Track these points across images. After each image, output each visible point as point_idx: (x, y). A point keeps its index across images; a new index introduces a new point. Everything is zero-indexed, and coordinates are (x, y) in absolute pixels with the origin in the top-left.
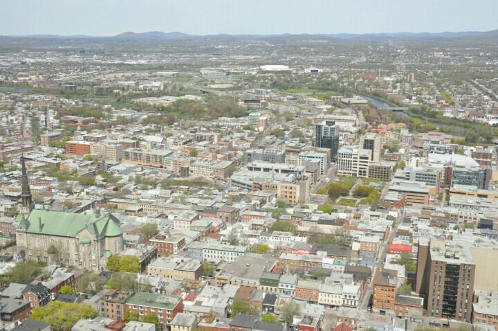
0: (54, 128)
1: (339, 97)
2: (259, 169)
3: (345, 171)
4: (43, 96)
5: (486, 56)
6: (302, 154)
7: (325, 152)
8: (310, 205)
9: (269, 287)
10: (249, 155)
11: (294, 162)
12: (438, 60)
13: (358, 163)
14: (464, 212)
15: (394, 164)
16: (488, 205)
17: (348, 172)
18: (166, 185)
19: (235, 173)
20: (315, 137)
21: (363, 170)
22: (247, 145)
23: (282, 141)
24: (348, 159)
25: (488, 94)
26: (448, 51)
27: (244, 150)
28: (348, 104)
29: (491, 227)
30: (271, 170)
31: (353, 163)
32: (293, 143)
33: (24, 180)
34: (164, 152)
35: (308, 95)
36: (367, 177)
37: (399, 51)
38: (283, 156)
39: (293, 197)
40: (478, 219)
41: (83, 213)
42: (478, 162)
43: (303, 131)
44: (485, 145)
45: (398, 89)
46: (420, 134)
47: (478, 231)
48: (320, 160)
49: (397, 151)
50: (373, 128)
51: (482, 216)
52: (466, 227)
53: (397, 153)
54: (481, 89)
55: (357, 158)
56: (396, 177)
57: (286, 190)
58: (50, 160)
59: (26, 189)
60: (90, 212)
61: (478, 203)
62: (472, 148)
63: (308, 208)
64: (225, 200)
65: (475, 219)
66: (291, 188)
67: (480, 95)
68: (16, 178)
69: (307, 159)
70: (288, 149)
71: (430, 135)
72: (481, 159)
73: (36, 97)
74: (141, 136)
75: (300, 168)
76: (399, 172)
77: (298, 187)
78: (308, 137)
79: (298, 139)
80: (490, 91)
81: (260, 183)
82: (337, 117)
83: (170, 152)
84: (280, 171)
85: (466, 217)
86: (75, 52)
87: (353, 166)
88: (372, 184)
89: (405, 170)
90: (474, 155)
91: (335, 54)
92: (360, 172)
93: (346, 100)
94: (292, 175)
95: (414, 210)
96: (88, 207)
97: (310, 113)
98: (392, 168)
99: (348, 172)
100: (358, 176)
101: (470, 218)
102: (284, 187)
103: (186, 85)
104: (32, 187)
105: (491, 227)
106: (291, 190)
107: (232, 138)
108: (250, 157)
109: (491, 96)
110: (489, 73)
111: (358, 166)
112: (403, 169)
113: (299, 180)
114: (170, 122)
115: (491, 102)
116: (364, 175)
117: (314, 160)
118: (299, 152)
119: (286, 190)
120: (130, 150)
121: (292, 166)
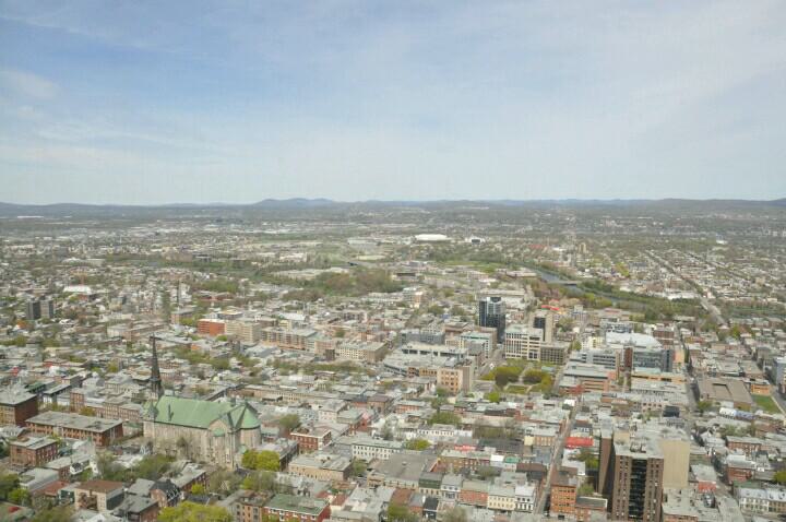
0: (185, 304)
2: (415, 352)
4: (175, 269)
6: (464, 334)
9: (430, 490)
10: (404, 335)
11: (455, 344)
12: (609, 229)
13: (528, 344)
14: (647, 399)
15: (568, 345)
16: (673, 390)
18: (310, 369)
19: (387, 357)
22: (400, 324)
25: (664, 266)
27: (398, 330)
28: (515, 278)
29: (677, 415)
32: (453, 321)
33: (154, 363)
34: (306, 333)
36: (538, 360)
38: (443, 337)
41: (216, 401)
42: (661, 341)
43: (464, 307)
45: (569, 261)
46: (596, 311)
47: (664, 420)
49: (571, 330)
51: (667, 403)
52: (651, 415)
54: (657, 261)
56: (572, 360)
58: (181, 340)
59: (156, 372)
60: (224, 399)
61: (662, 388)
62: (653, 326)
63: (472, 396)
64: (376, 388)
66: (452, 373)
68: (144, 360)
69: (470, 340)
73: (168, 270)
74: (280, 314)
76: (574, 355)
77: (461, 373)
79: (458, 317)
80: (667, 263)
81: (417, 368)
83: (313, 332)
86: (212, 221)
88: (544, 368)
89: (582, 352)
90: (655, 334)
93: (512, 273)
94: (453, 359)
95: (592, 398)
96: (221, 394)
98: (566, 351)
103: (331, 257)
104: (161, 370)
105: (677, 415)
107: (383, 316)
108: (404, 339)
109: (668, 269)
110: (666, 244)
112: (578, 350)
113: (462, 364)
114: (314, 298)
115: (669, 275)
117: (477, 341)
118: (460, 332)
120: (268, 329)
121: (453, 348)
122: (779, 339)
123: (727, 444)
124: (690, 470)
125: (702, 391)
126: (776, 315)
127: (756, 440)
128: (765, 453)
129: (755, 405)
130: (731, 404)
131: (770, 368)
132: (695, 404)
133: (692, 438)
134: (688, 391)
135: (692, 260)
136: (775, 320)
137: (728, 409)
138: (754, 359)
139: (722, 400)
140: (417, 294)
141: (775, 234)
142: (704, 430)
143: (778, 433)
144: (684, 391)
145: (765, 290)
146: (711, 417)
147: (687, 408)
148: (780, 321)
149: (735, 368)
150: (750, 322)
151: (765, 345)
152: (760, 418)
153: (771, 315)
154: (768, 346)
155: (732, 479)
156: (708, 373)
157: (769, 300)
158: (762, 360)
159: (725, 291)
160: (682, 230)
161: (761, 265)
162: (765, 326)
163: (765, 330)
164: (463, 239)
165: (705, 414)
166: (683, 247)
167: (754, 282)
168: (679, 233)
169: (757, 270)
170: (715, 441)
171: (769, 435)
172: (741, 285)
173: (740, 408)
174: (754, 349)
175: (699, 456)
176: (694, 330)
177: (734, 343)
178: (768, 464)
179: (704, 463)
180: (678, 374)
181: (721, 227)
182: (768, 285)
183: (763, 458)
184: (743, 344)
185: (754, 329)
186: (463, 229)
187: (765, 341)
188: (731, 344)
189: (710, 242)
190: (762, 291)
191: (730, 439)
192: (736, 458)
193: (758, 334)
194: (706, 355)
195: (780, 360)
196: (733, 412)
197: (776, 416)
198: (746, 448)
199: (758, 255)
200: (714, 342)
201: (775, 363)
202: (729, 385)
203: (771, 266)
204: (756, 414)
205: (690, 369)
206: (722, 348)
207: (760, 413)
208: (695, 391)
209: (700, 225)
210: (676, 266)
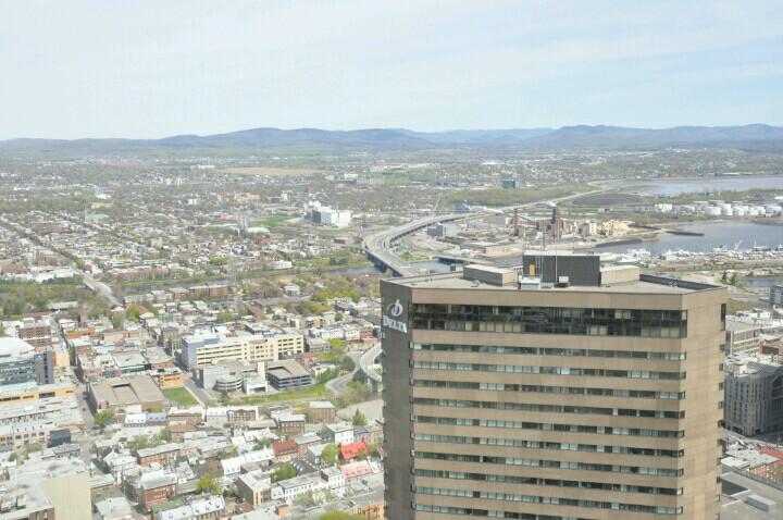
5: (12, 178)
14: (24, 428)
16: (58, 407)
25: (26, 236)
29: (68, 440)
40: (47, 433)
44: (38, 314)
47: (49, 452)
51: (52, 427)
52: (29, 451)
54: (13, 229)
62: (17, 323)
65: (42, 434)
67: (13, 237)
80: (28, 231)
85: (26, 436)
101: (34, 435)
105: (68, 440)
109: (32, 239)
110: (22, 203)
115: (34, 248)
122: (186, 313)
123: (139, 462)
124: (95, 510)
125: (100, 400)
126: (180, 283)
127: (174, 446)
128: (185, 459)
129: (167, 403)
130: (139, 407)
131: (180, 351)
132: (91, 419)
133: (93, 466)
134: (80, 403)
135: (66, 224)
136: (179, 290)
137: (136, 414)
138: (160, 343)
139: (127, 405)
141: (169, 182)
142: (107, 451)
143: (198, 429)
144: (75, 404)
145: (164, 254)
146: (115, 431)
147: (81, 427)
148: (184, 291)
149: (139, 360)
150: (150, 297)
151: (171, 324)
153: (174, 285)
154: (174, 324)
155: (150, 504)
156: (105, 374)
157: (170, 266)
158: (170, 343)
159: (115, 261)
160: (47, 183)
161: (156, 223)
162: (168, 300)
163: (168, 304)
165: (109, 428)
166: (52, 207)
167: (149, 246)
168: (41, 187)
169: (151, 230)
170: (123, 462)
171: (187, 435)
172: (134, 252)
173: (150, 411)
174: (158, 331)
175: (106, 488)
176: (79, 320)
177: (132, 327)
178: (191, 472)
179: (112, 495)
180: (63, 384)
181: (100, 176)
182: (166, 247)
183: (184, 465)
184: (144, 327)
185: (155, 305)
187: (170, 319)
188: (130, 329)
189: (86, 197)
190: (160, 256)
191: (141, 453)
192: (153, 475)
193: (162, 312)
194: (99, 350)
195: (189, 340)
196: (143, 417)
197: (192, 410)
198: (164, 460)
199: (150, 210)
200: (107, 331)
202: (133, 385)
203: (167, 223)
204: (170, 413)
205: (79, 373)
206: (118, 337)
207: (174, 410)
208: (89, 400)
209: (71, 175)
210: (43, 235)
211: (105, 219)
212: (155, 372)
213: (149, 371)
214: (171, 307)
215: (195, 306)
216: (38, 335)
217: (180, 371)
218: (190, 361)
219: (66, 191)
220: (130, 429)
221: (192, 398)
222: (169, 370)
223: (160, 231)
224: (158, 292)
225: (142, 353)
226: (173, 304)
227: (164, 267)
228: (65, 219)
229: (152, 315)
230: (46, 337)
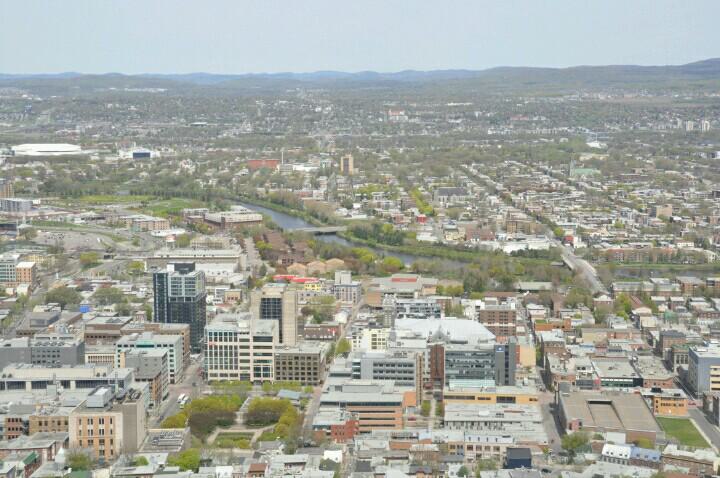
1: (200, 210)
2: (21, 385)
3: (224, 371)
5: (487, 119)
6: (124, 340)
7: (177, 333)
8: (148, 457)
11: (108, 360)
12: (396, 126)
13: (251, 351)
14: (475, 437)
15: (325, 346)
16: (517, 418)
17: (229, 371)
20: (152, 300)
21: (262, 365)
23: (77, 314)
24: (229, 344)
25: (496, 192)
26: (417, 109)
28: (221, 225)
30: (50, 383)
31: (240, 351)
32: (106, 315)
35: (132, 208)
36: (272, 379)
37: (318, 109)
38: (81, 349)
39: (107, 442)
40: (503, 449)
43: (124, 287)
45: (323, 190)
46: (375, 280)
48: (165, 350)
49: (331, 319)
50: (277, 272)
51: (509, 441)
52: (482, 468)
53: (331, 324)
54: (482, 183)
55: (248, 340)
56: (333, 375)
57: (90, 427)
62: (478, 302)
63: (144, 462)
65: (498, 449)
66: (101, 421)
67: (482, 194)
69: (136, 351)
70: (91, 331)
71: (394, 280)
72: (497, 324)
75: (123, 373)
76: (339, 364)
77: (118, 417)
78: (136, 301)
79: (112, 307)
80: (500, 186)
81: (25, 418)
82: (200, 253)
84: (73, 384)
87: (240, 358)
89: (351, 358)
91: (186, 117)
92: (257, 369)
93: (217, 216)
94: (102, 391)
95: (374, 442)
97: (137, 249)
98: (323, 356)
99: (229, 371)
100: (252, 379)
101: (487, 448)
102: (84, 422)
106: (101, 427)
109: (503, 197)
110: (496, 151)
111: (252, 358)
112: (345, 355)
113: (121, 400)
115: (506, 208)
116: (266, 375)
117: (151, 353)
118: (116, 337)
119: (90, 427)
121: (102, 370)
122: (699, 314)
125: (570, 418)
126: (692, 272)
130: (622, 437)
131: (685, 367)
132: (559, 441)
134: (546, 419)
135: (545, 179)
136: (689, 280)
138: (658, 352)
139: (605, 431)
140: (22, 265)
141: (690, 126)
144: (538, 417)
145: (673, 227)
146: (588, 463)
147: (544, 449)
148: (699, 282)
149: (626, 371)
150: (648, 287)
151: (675, 327)
152: (671, 458)
153: (684, 273)
154: (680, 328)
156: (581, 384)
157: (680, 245)
158: (671, 353)
159: (604, 232)
160: (527, 126)
161: (665, 185)
162: (674, 293)
163: (673, 299)
164: (114, 152)
165: (579, 457)
166: (529, 157)
167: (653, 215)
168: (520, 130)
169: (658, 193)
172: (631, 222)
173: (636, 444)
174: (656, 334)
176: (552, 308)
177: (621, 325)
180: (526, 388)
181: (592, 116)
182: (676, 218)
184: (637, 326)
185: (654, 298)
186: (115, 133)
187: (675, 320)
189: (574, 145)
190: (668, 231)
193: (663, 308)
194: (574, 349)
195: (702, 352)
196: (626, 451)
197: (699, 454)
199: (659, 165)
200: (588, 326)
201: (696, 359)
202: (615, 402)
203: (683, 184)
204: (666, 451)
205: (547, 378)
206: (600, 336)
207: (672, 449)
208: (557, 413)
209: (558, 115)
210: (517, 192)
211: (595, 175)
212: (647, 392)
213: (639, 389)
214: (678, 303)
215: (713, 305)
216: (501, 321)
217: (684, 395)
218: (701, 383)
219: (549, 137)
220: (606, 464)
221: (700, 435)
222: (669, 392)
223: (670, 196)
224: (661, 281)
225: (632, 362)
226: (681, 299)
227: (672, 246)
228: (545, 173)
229: (649, 311)
230: (510, 325)
